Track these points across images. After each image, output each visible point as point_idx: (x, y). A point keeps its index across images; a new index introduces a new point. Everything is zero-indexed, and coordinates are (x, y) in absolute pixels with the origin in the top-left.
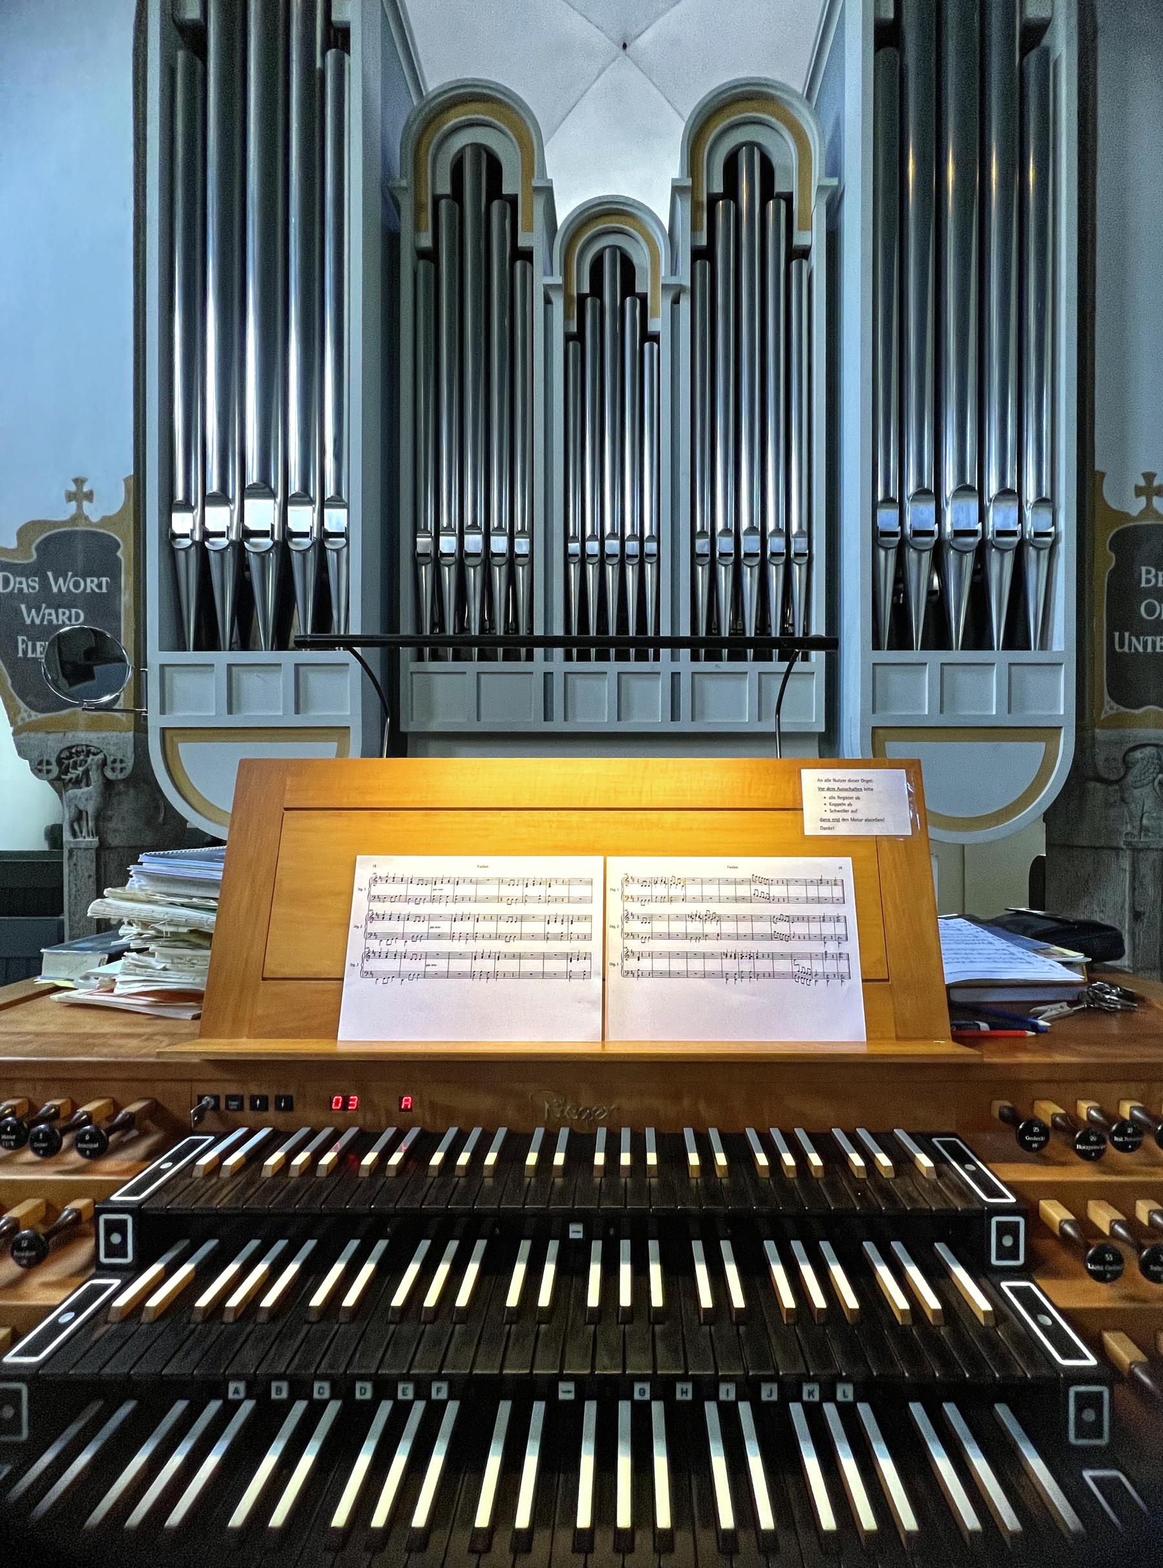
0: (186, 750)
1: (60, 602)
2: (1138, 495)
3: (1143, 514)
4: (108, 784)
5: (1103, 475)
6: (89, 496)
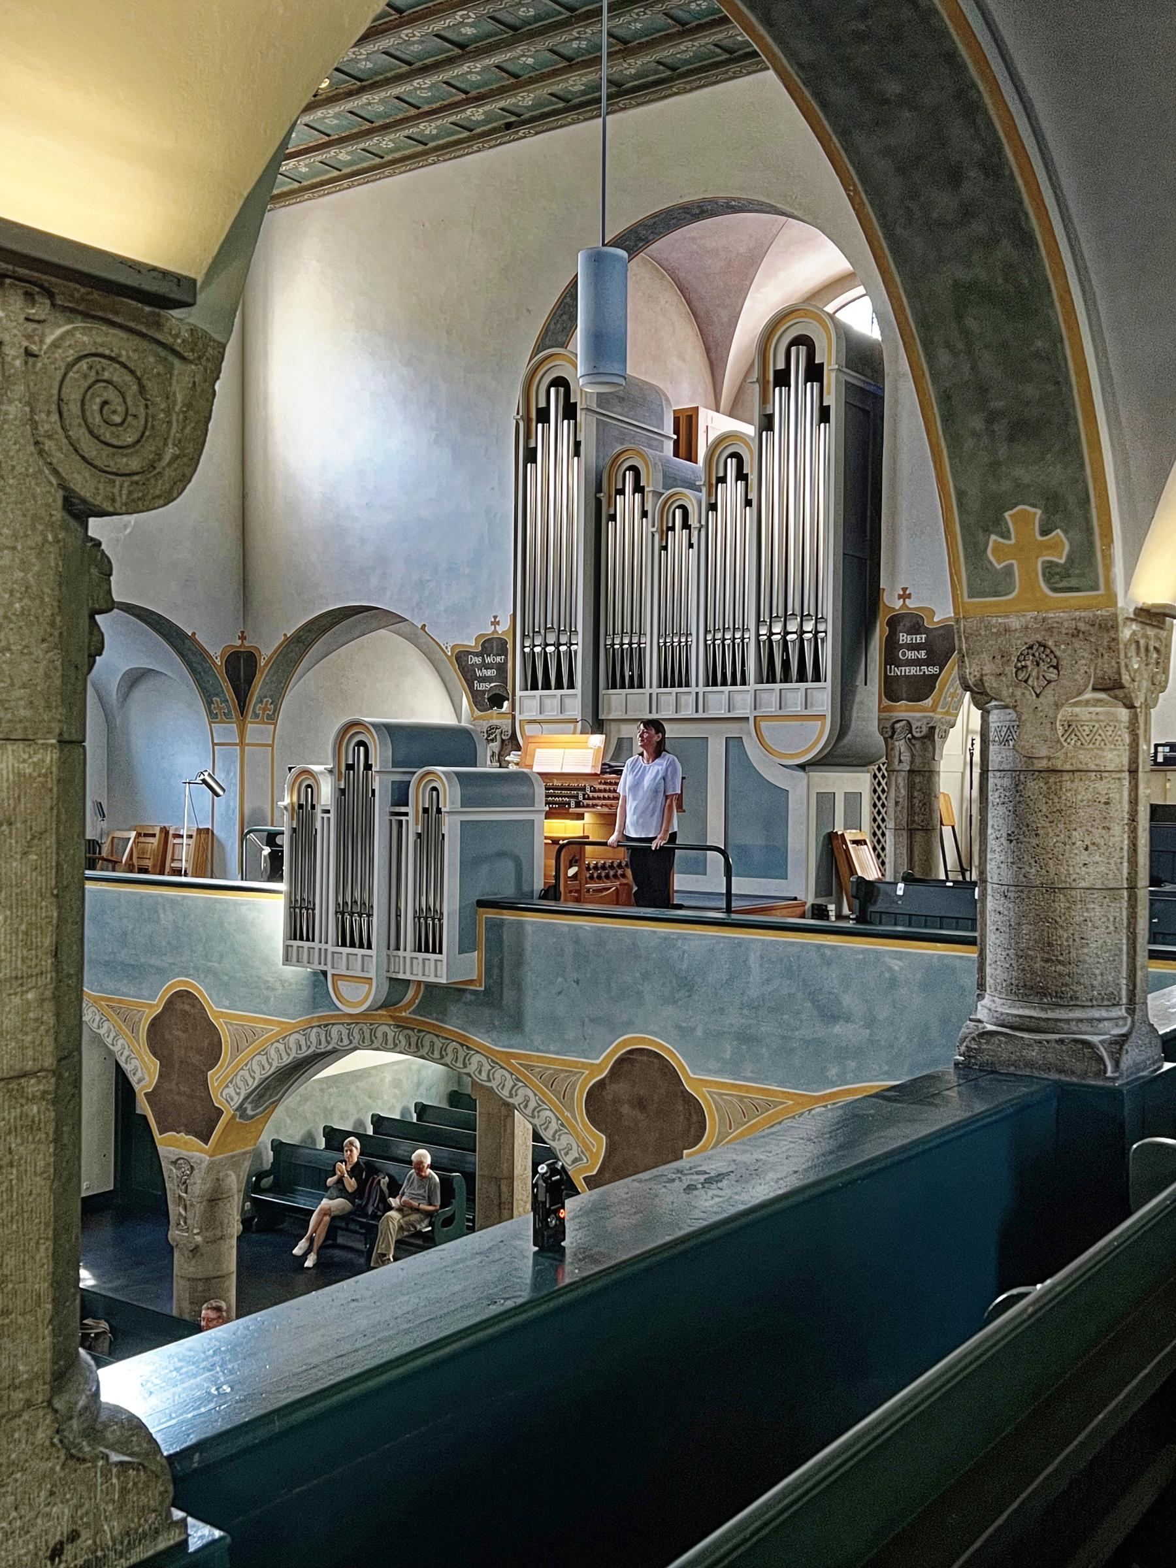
0: (527, 727)
1: (488, 667)
4: (503, 741)
6: (498, 623)
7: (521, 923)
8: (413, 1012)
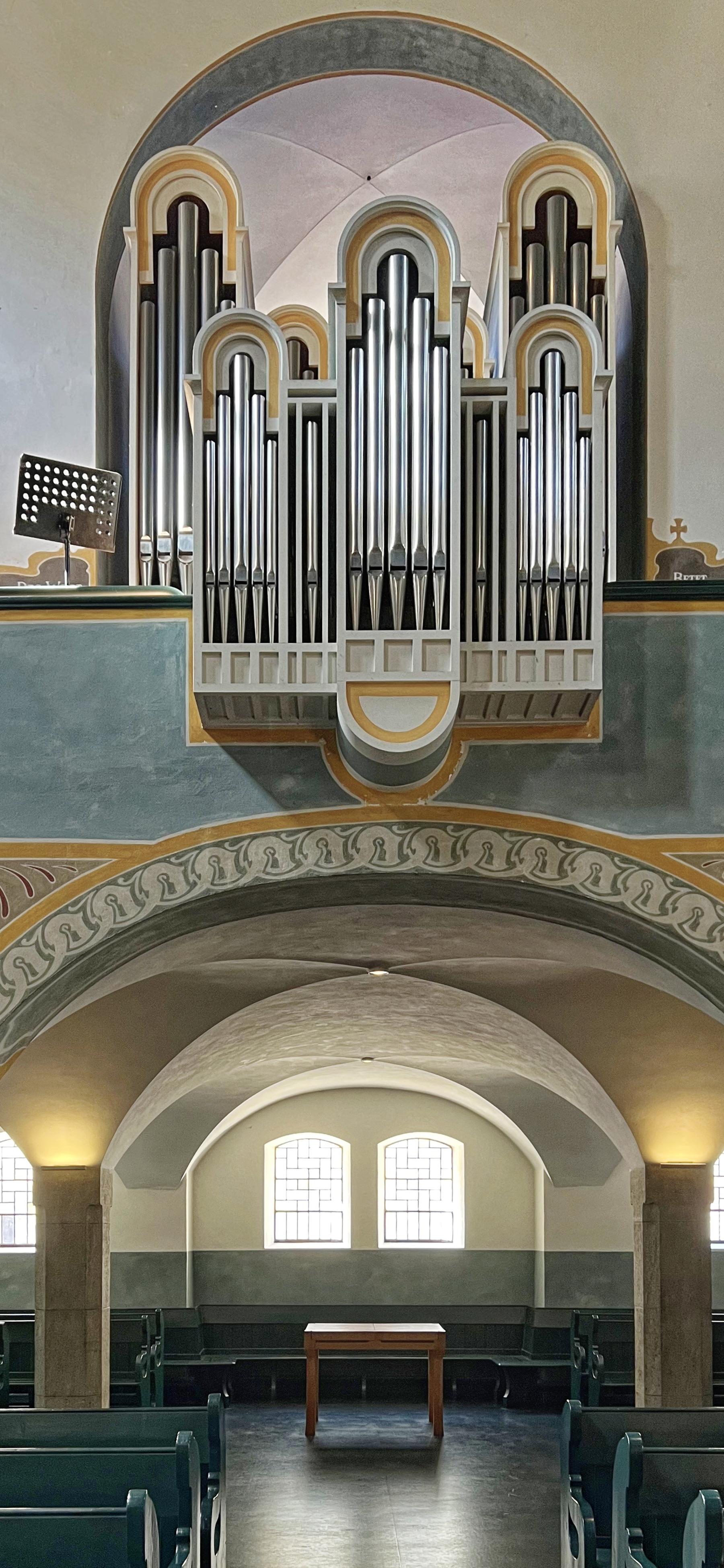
2: (672, 532)
3: (675, 542)
5: (652, 520)
7: (682, 622)
8: (444, 797)
